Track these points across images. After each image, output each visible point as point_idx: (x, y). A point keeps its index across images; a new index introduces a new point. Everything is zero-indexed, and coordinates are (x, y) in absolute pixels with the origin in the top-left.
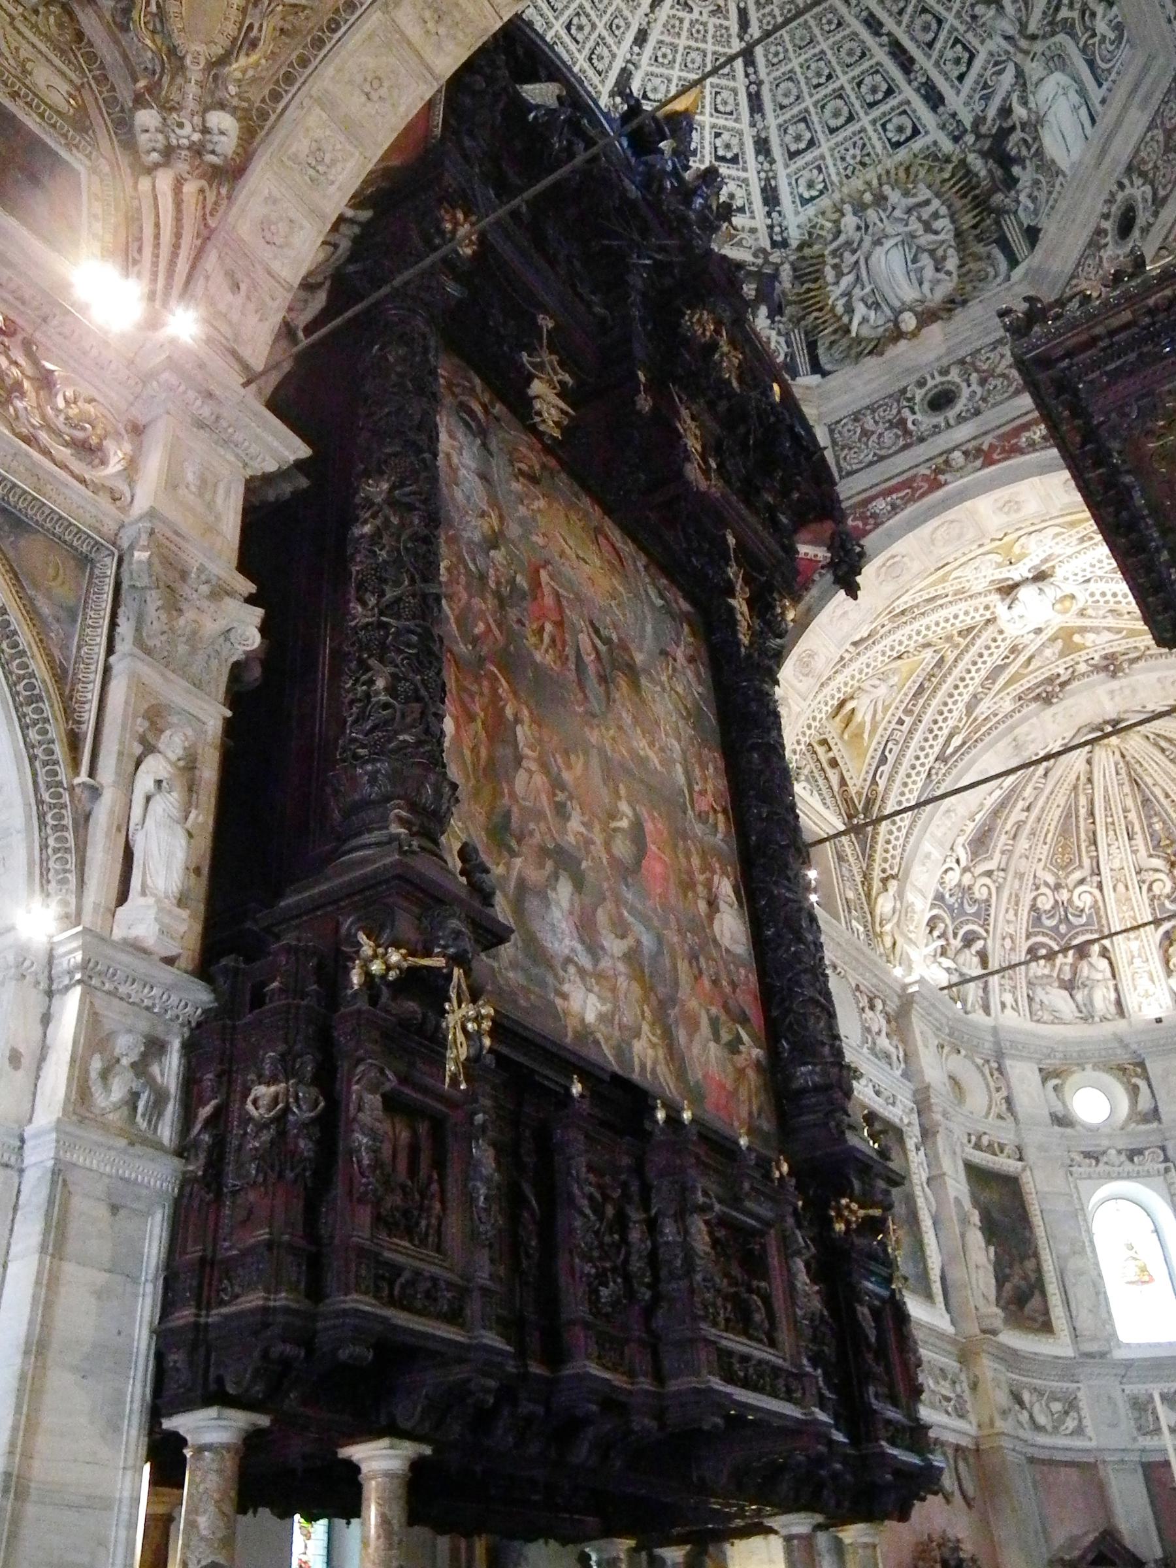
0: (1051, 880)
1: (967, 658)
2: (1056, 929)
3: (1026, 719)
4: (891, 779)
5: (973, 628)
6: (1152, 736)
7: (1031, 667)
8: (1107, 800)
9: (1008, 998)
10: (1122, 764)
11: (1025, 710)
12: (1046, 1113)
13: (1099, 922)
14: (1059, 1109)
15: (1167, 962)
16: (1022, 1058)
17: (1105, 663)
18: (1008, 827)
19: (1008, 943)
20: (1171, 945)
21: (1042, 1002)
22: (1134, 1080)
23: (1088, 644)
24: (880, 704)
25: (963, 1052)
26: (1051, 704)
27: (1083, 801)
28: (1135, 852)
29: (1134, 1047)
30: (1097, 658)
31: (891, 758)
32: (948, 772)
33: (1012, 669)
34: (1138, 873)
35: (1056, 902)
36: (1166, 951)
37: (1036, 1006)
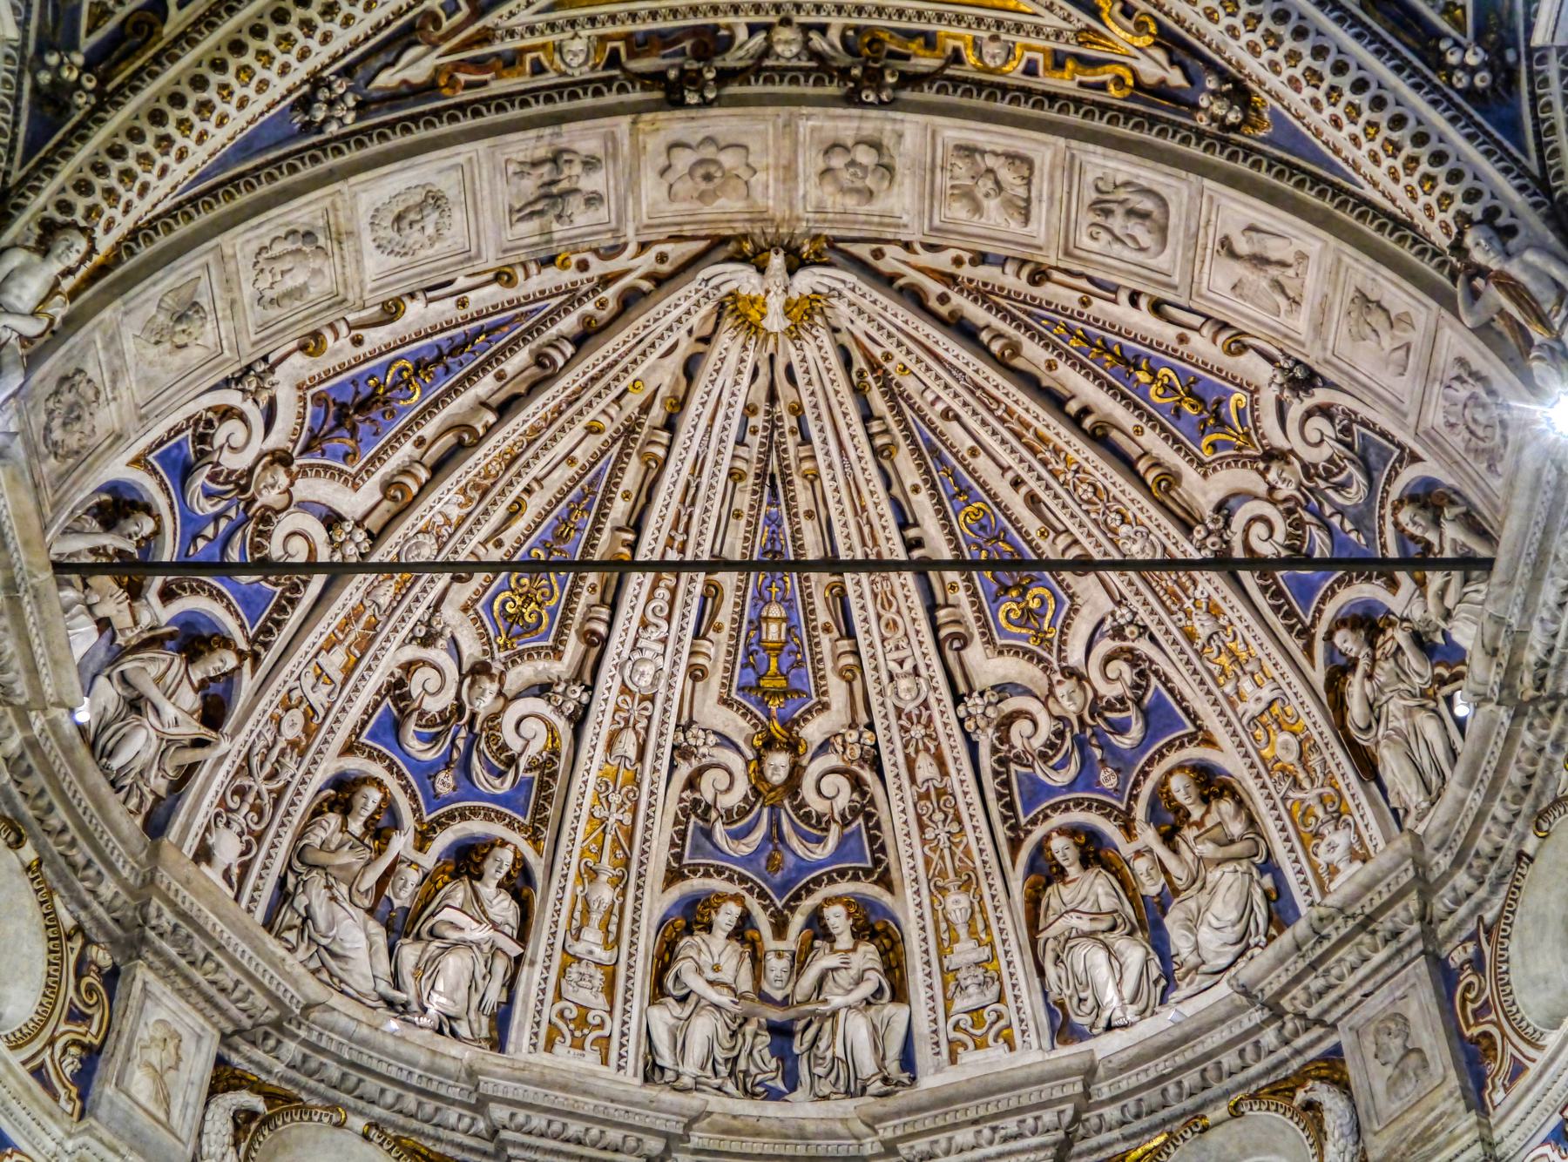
0: (472, 649)
2: (428, 772)
6: (859, 362)
8: (689, 496)
9: (228, 848)
10: (758, 421)
11: (611, 98)
13: (539, 808)
16: (189, 989)
17: (844, 60)
18: (429, 430)
19: (293, 727)
21: (308, 917)
25: (28, 853)
26: (680, 104)
27: (631, 477)
28: (697, 674)
29: (499, 1113)
30: (837, 22)
34: (683, 728)
35: (459, 709)
37: (287, 916)
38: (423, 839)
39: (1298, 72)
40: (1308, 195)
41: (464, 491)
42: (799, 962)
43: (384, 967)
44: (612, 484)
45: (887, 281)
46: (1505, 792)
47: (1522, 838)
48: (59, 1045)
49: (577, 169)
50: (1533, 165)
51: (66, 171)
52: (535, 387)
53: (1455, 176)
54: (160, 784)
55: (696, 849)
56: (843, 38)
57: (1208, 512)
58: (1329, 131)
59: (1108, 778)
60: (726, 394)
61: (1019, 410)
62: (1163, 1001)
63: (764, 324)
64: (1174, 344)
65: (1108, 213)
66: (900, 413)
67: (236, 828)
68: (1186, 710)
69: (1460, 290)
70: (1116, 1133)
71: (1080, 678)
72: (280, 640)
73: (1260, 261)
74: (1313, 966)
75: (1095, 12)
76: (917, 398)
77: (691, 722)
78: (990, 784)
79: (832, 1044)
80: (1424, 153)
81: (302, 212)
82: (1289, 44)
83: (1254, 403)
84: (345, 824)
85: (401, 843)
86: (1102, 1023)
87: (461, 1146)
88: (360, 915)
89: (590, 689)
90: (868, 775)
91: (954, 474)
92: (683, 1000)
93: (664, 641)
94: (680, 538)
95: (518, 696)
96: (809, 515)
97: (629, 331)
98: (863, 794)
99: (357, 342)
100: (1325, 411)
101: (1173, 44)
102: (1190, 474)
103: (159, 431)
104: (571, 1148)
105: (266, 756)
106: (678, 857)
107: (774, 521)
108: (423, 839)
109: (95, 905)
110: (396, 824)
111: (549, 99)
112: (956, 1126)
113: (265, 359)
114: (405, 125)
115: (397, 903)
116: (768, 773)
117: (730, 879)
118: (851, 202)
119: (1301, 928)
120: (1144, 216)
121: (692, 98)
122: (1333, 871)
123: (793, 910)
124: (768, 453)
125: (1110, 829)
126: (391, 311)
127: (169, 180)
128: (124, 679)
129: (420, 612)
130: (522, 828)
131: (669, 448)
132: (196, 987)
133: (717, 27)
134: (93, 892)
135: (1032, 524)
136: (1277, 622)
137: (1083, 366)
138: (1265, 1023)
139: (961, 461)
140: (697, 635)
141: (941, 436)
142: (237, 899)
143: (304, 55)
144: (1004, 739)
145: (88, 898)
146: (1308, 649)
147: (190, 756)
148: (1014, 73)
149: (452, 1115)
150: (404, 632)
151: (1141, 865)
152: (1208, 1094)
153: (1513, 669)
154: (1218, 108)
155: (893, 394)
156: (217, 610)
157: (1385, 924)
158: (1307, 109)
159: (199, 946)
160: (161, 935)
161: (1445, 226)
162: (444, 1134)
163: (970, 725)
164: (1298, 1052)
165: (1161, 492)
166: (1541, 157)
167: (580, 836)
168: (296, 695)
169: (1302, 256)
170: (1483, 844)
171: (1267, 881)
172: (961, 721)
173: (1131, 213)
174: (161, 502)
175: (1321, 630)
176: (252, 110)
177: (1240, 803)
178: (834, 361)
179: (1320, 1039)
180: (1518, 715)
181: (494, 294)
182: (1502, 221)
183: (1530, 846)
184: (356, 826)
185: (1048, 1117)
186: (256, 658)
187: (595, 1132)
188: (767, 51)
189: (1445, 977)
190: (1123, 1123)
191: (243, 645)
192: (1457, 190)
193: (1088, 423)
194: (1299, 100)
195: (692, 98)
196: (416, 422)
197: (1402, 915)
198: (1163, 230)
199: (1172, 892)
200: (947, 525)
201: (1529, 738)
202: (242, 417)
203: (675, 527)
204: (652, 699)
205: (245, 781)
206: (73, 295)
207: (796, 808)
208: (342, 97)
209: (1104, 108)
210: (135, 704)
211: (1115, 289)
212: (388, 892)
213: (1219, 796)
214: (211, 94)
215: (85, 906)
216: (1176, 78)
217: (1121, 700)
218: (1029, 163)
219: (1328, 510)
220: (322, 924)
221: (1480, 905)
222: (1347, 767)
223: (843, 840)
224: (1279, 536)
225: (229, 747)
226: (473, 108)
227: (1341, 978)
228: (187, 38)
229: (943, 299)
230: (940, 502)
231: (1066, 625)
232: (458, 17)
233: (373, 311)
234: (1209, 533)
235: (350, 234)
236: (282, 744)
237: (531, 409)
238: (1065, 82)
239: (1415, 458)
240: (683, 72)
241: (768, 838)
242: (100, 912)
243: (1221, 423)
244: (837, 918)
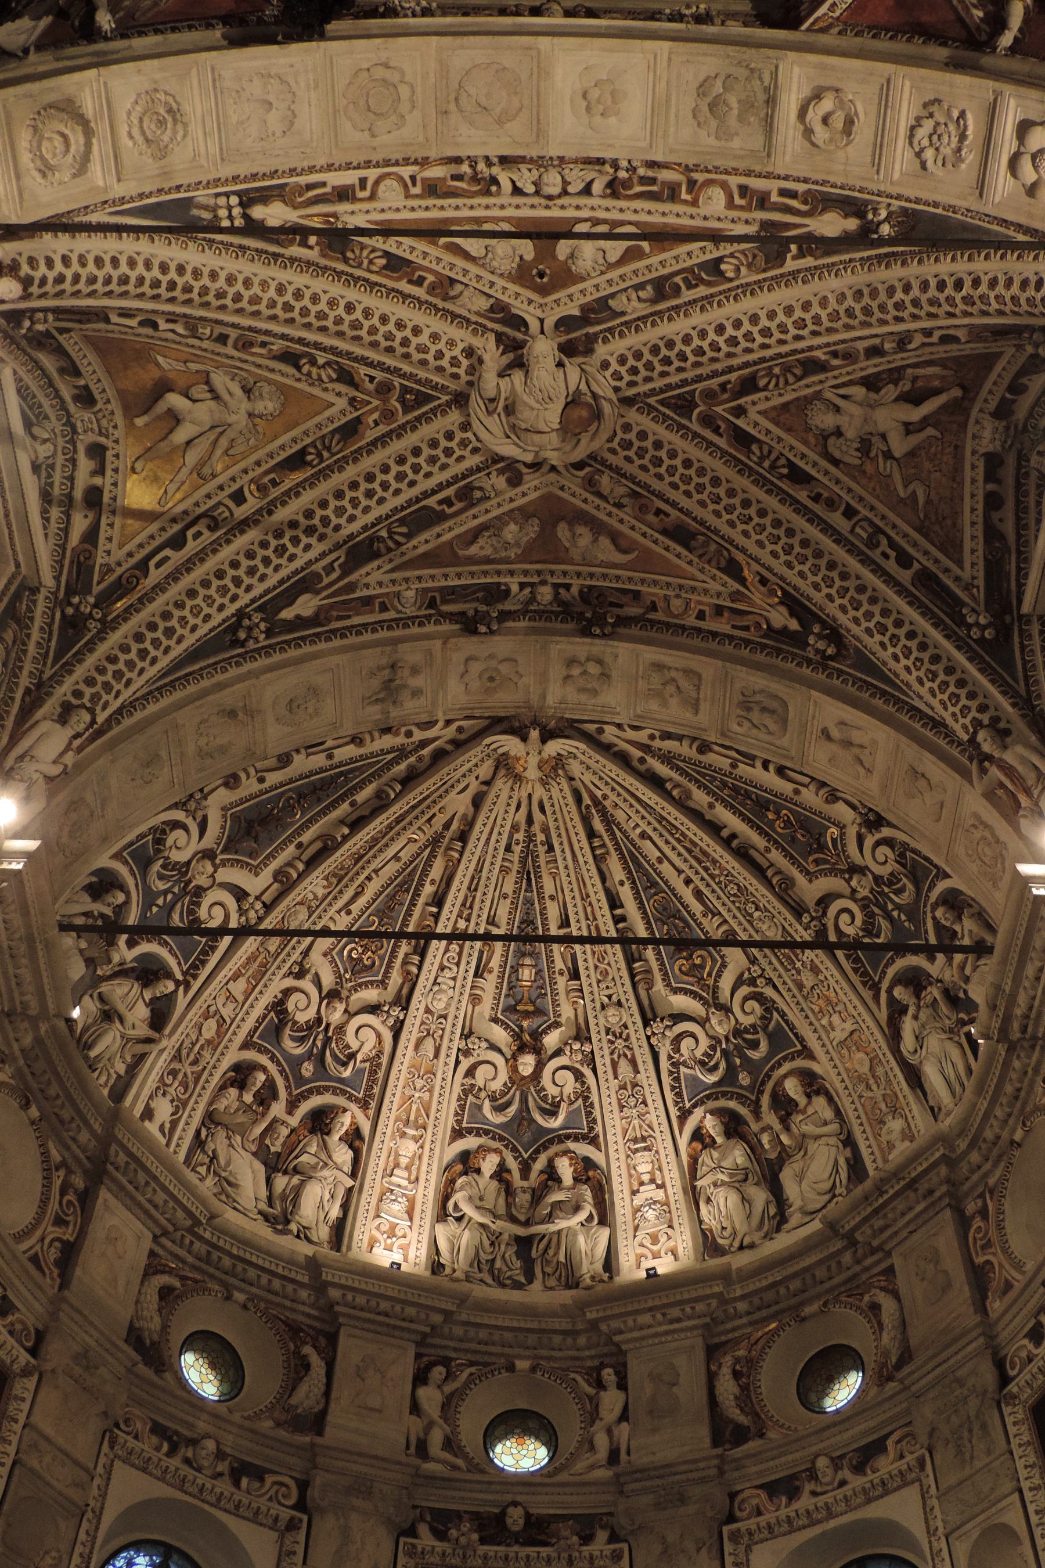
0: (328, 980)
1: (398, 446)
2: (296, 1063)
3: (428, 637)
4: (174, 577)
5: (429, 398)
6: (587, 800)
7: (473, 550)
9: (163, 1110)
10: (520, 836)
11: (429, 628)
12: (126, 1314)
14: (153, 1324)
15: (446, 1198)
18: (306, 837)
19: (210, 1029)
20: (466, 1173)
21: (214, 1158)
22: (307, 1350)
23: (575, 554)
24: (224, 442)
25: (34, 1112)
26: (475, 632)
27: (437, 871)
28: (475, 1000)
29: (334, 1293)
30: (576, 584)
31: (192, 546)
32: (267, 651)
33: (449, 532)
34: (467, 1035)
35: (319, 1020)
36: (452, 1182)
38: (292, 1106)
39: (871, 625)
40: (878, 702)
41: (326, 878)
42: (537, 1196)
43: (263, 1193)
44: (425, 873)
45: (606, 749)
46: (1004, 1100)
47: (1013, 1131)
48: (47, 1241)
49: (406, 672)
50: (1022, 689)
51: (80, 671)
52: (376, 812)
53: (972, 696)
54: (121, 1068)
55: (471, 1116)
56: (581, 592)
57: (811, 905)
58: (892, 663)
59: (744, 1078)
60: (499, 821)
61: (690, 835)
62: (778, 1230)
63: (526, 774)
64: (791, 795)
65: (749, 709)
66: (613, 834)
67: (169, 1097)
68: (796, 1035)
69: (974, 768)
70: (745, 1320)
71: (726, 1010)
72: (204, 974)
73: (847, 744)
74: (876, 1211)
75: (742, 581)
76: (623, 825)
77: (471, 1033)
78: (666, 1080)
79: (556, 1254)
80: (952, 680)
81: (228, 697)
82: (865, 607)
83: (842, 835)
84: (241, 1095)
85: (278, 1109)
86: (736, 1244)
87: (308, 1315)
88: (248, 1156)
89: (405, 1008)
90: (587, 1071)
91: (646, 874)
92: (459, 1219)
93: (454, 979)
94: (466, 913)
95: (356, 1013)
96: (552, 898)
97: (437, 777)
98: (583, 1083)
99: (261, 780)
100: (888, 842)
101: (793, 603)
102: (800, 879)
103: (131, 836)
104: (381, 1318)
105: (191, 1050)
106: (459, 1122)
107: (529, 902)
108: (292, 1106)
109: (74, 1147)
110: (275, 1096)
111: (390, 628)
112: (638, 1312)
113: (201, 790)
114: (298, 643)
115: (273, 1149)
116: (520, 1068)
117: (493, 1138)
118: (583, 698)
119: (868, 1184)
120: (773, 712)
121: (483, 629)
122: (891, 1146)
123: (534, 1160)
124: (526, 858)
125: (744, 1111)
126: (285, 760)
127: (146, 676)
128: (101, 998)
129: (296, 956)
130: (357, 1100)
131: (461, 854)
132: (140, 1205)
133: (499, 584)
134: (74, 1139)
135: (697, 907)
136: (855, 979)
137: (732, 807)
138: (845, 1249)
139: (652, 866)
140: (476, 975)
141: (638, 849)
142: (168, 1145)
143: (234, 598)
144: (677, 1050)
145: (70, 1143)
146: (876, 998)
147: (140, 1048)
148: (691, 621)
149: (304, 1294)
150: (284, 970)
151: (765, 1139)
152: (807, 1295)
153: (1007, 1019)
154: (821, 645)
155: (609, 821)
156: (163, 953)
157: (923, 1186)
158: (877, 648)
159: (142, 1177)
160: (117, 1169)
161: (965, 727)
162: (302, 1308)
163: (654, 1041)
164: (867, 1269)
165: (784, 890)
166: (1027, 684)
167: (395, 1107)
168: (212, 1009)
169: (874, 742)
170: (989, 1134)
171: (848, 1152)
172: (648, 1038)
173: (764, 709)
174: (130, 882)
175: (885, 985)
176: (200, 632)
177: (830, 1100)
178: (570, 799)
179: (880, 1261)
180: (1012, 1048)
181: (350, 751)
182: (1002, 725)
183: (1018, 1136)
184: (248, 1098)
185: (700, 1307)
186: (188, 986)
187: (398, 1308)
188: (533, 599)
189: (963, 1223)
190: (749, 1313)
191: (179, 976)
192: (973, 704)
193: (735, 843)
194: (872, 643)
195: (483, 629)
196: (299, 832)
197: (935, 1180)
198: (784, 722)
199: (784, 1156)
200: (641, 907)
201: (1017, 1064)
202: (185, 828)
203: (464, 905)
204: (445, 1017)
205: (176, 1065)
206: (80, 749)
207: (538, 1092)
208: (257, 625)
209: (747, 642)
210: (109, 1015)
211: (753, 758)
212: (268, 1142)
213: (818, 1093)
214: (174, 622)
215: (68, 1148)
216: (794, 625)
217: (753, 1026)
218: (699, 677)
219: (890, 907)
220: (222, 1162)
221: (986, 1175)
222: (900, 1077)
223: (569, 1114)
224: (858, 922)
225: (169, 1044)
226: (342, 632)
227: (895, 1220)
228: (160, 588)
229: (642, 760)
230: (638, 892)
231: (719, 976)
232: (334, 576)
233: (272, 762)
234: (813, 919)
235: (259, 711)
236: (202, 1041)
237: (372, 826)
238: (722, 626)
239: (947, 876)
240: (476, 611)
241: (520, 1111)
242: (78, 1152)
243: (822, 847)
244: (565, 1169)
